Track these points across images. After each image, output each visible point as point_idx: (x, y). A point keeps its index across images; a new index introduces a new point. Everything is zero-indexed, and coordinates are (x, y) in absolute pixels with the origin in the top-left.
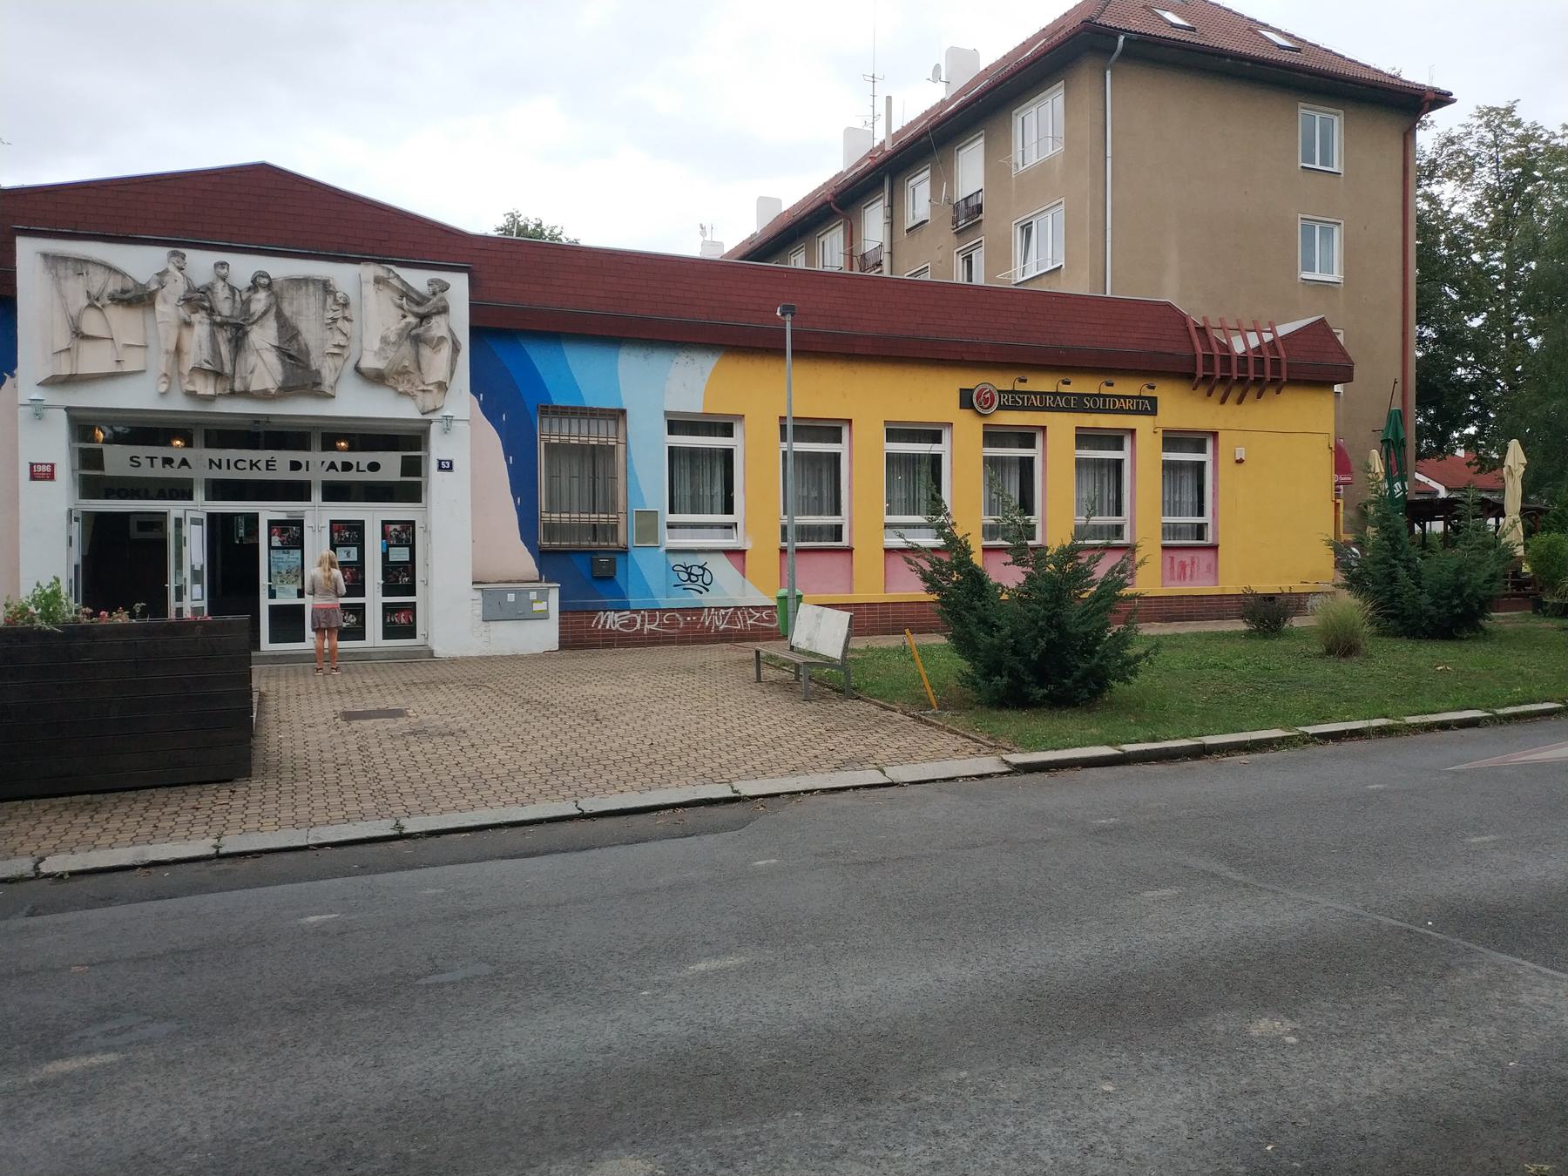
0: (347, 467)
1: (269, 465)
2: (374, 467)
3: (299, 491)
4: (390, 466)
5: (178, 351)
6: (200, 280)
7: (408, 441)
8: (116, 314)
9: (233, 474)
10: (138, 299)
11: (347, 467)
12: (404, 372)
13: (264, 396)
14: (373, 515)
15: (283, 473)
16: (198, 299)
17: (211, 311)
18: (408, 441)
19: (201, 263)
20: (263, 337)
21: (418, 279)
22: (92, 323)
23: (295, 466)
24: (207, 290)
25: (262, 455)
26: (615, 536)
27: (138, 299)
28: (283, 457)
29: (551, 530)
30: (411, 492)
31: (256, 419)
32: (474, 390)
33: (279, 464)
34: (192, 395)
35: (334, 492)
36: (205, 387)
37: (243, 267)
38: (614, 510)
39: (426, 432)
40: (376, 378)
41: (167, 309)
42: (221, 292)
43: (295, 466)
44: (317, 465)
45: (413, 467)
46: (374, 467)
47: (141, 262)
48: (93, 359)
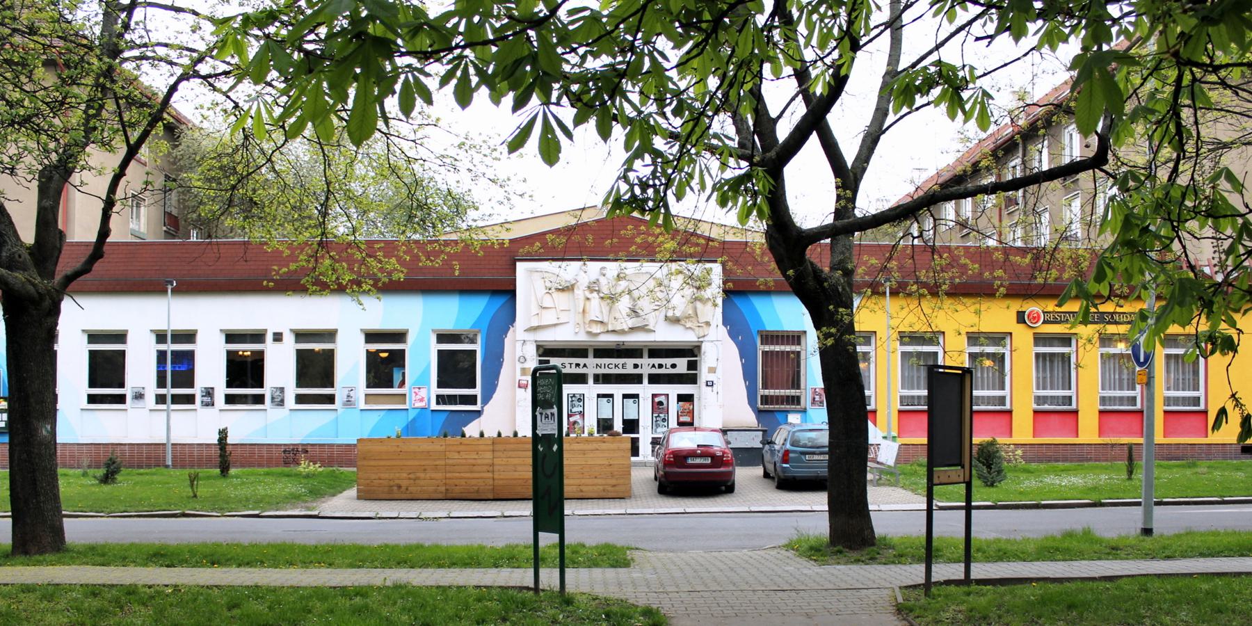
0: (660, 366)
1: (624, 366)
2: (674, 366)
3: (637, 379)
4: (682, 365)
5: (584, 311)
6: (593, 279)
7: (691, 352)
8: (556, 295)
9: (607, 371)
10: (568, 289)
11: (660, 366)
12: (689, 317)
13: (622, 332)
14: (674, 390)
15: (630, 370)
16: (593, 287)
17: (598, 291)
18: (691, 352)
19: (594, 267)
20: (624, 304)
21: (697, 269)
22: (547, 302)
23: (636, 366)
24: (596, 282)
25: (620, 361)
26: (799, 403)
27: (568, 289)
28: (630, 362)
29: (766, 400)
30: (691, 379)
31: (618, 344)
32: (725, 324)
33: (627, 366)
34: (589, 333)
35: (654, 379)
36: (596, 329)
37: (612, 268)
38: (799, 388)
39: (699, 347)
40: (676, 321)
41: (580, 292)
42: (603, 281)
43: (636, 366)
44: (646, 365)
45: (693, 366)
46: (674, 366)
47: (570, 270)
48: (548, 318)
